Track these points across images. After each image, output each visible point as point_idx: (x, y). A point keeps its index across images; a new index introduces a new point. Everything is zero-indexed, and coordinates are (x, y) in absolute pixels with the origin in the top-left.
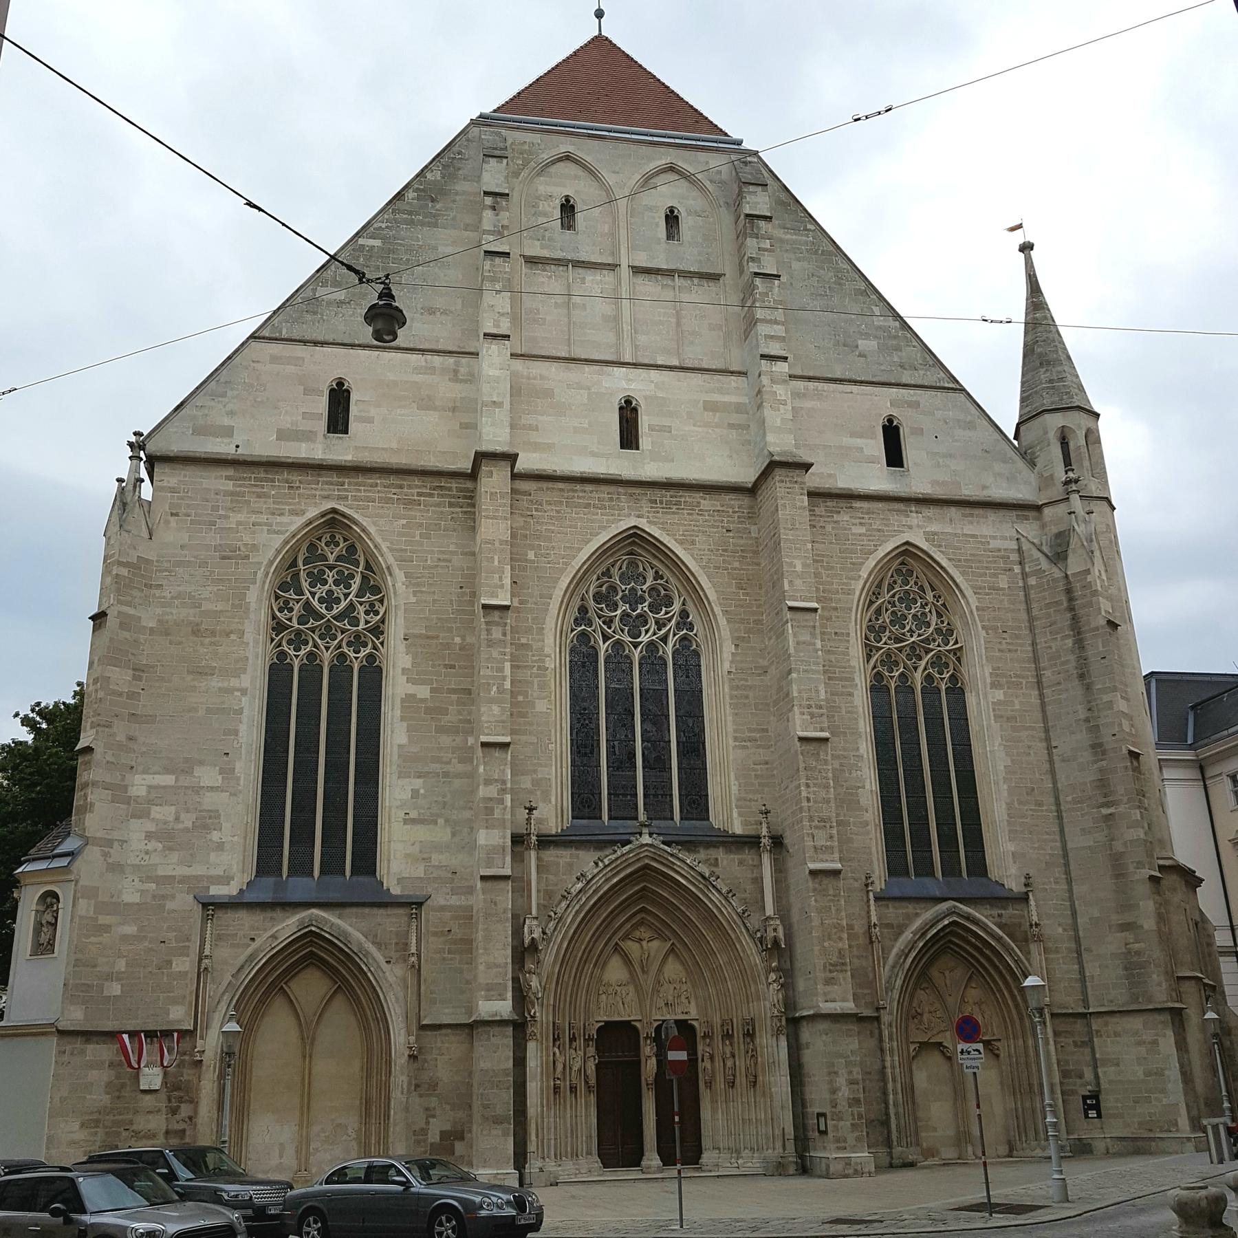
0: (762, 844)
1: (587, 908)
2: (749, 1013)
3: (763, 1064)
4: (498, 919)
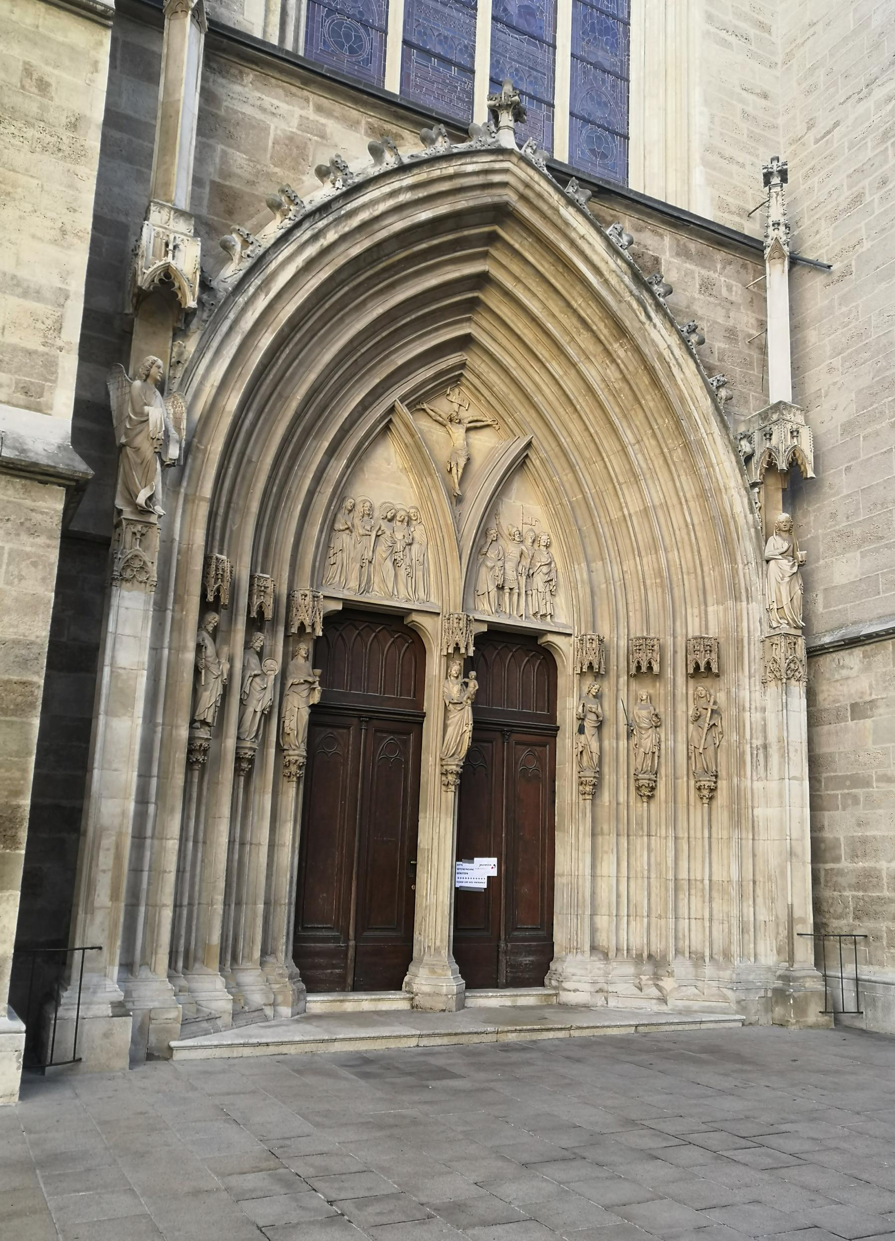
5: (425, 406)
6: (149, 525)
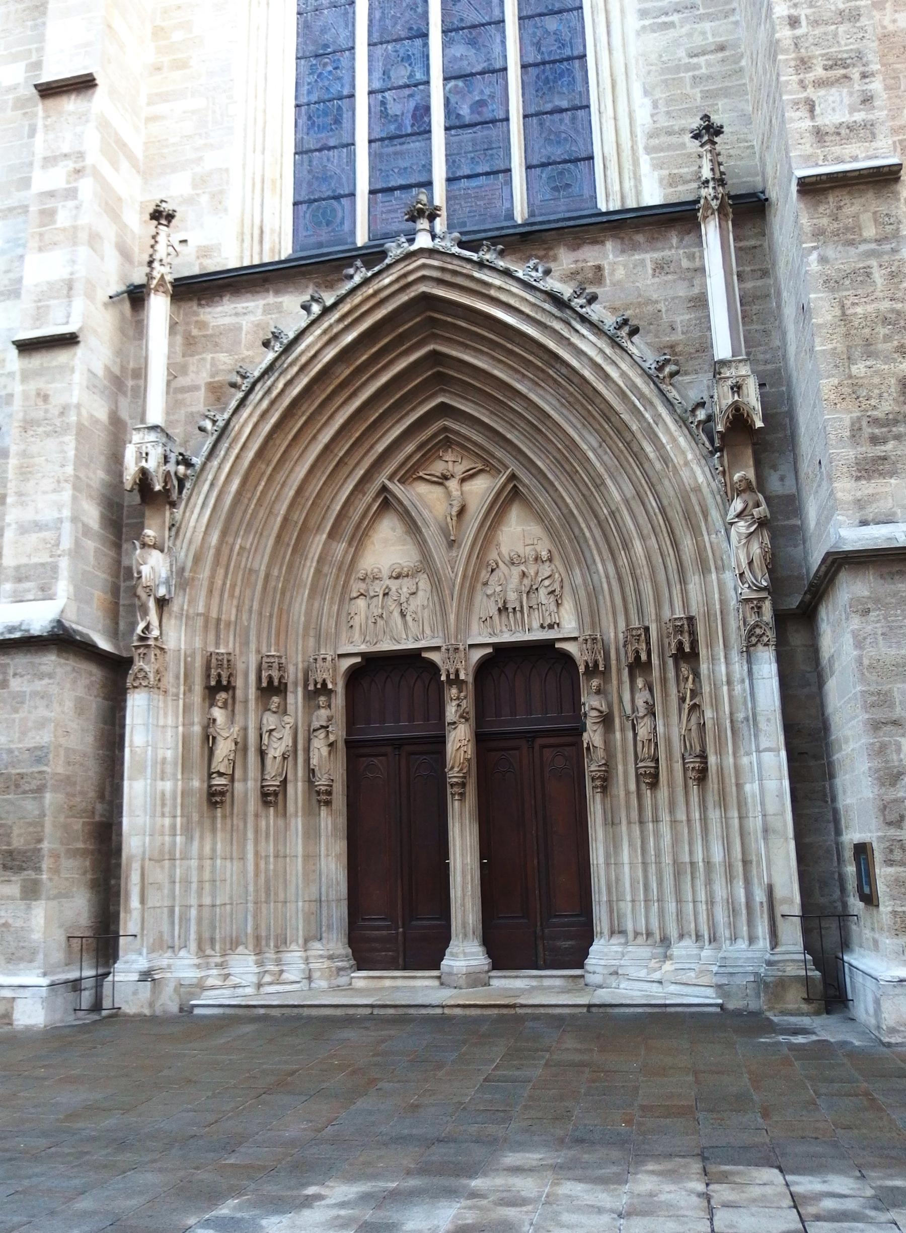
0: (702, 201)
1: (286, 401)
2: (686, 605)
3: (718, 723)
4: (49, 428)
5: (421, 474)
6: (148, 646)
